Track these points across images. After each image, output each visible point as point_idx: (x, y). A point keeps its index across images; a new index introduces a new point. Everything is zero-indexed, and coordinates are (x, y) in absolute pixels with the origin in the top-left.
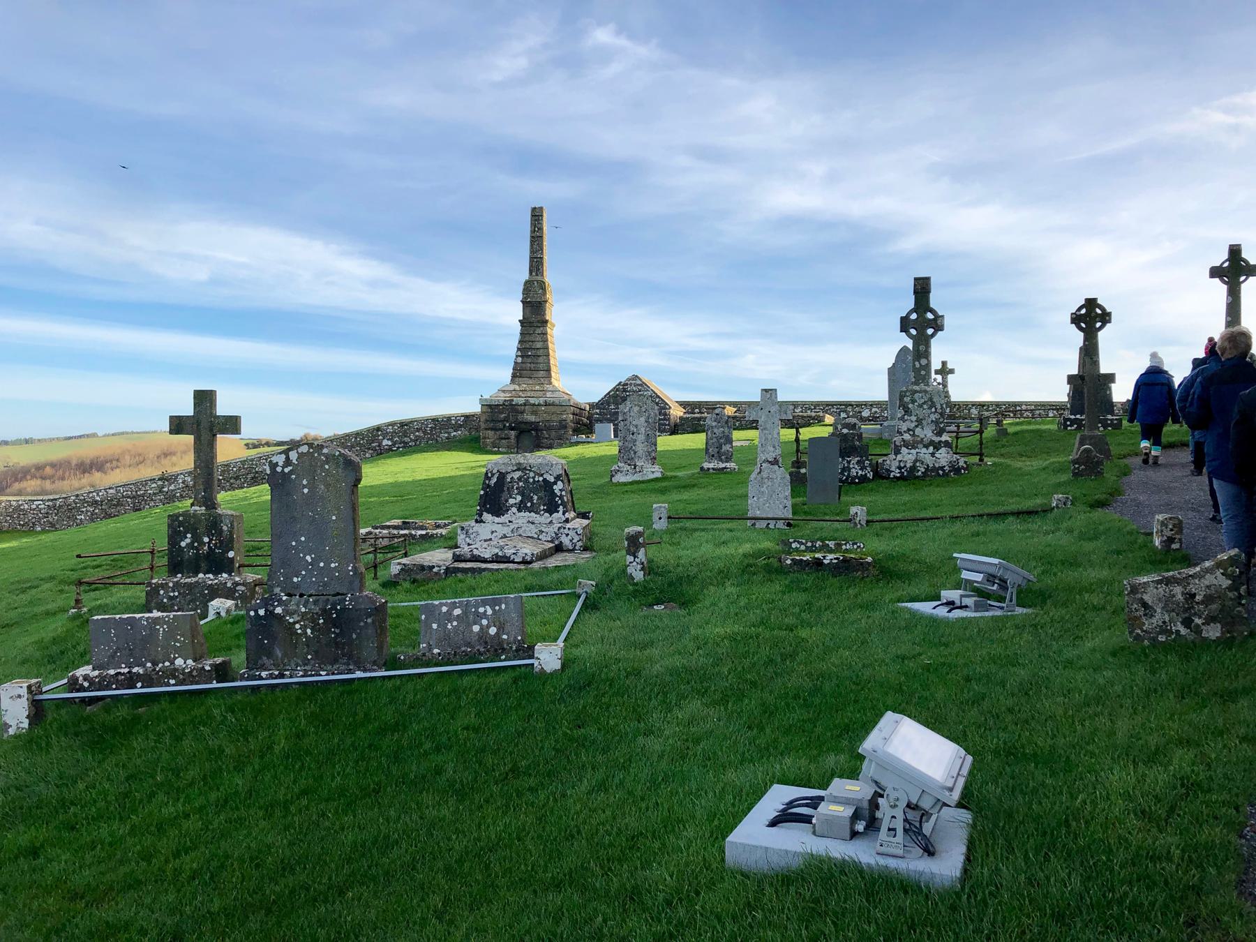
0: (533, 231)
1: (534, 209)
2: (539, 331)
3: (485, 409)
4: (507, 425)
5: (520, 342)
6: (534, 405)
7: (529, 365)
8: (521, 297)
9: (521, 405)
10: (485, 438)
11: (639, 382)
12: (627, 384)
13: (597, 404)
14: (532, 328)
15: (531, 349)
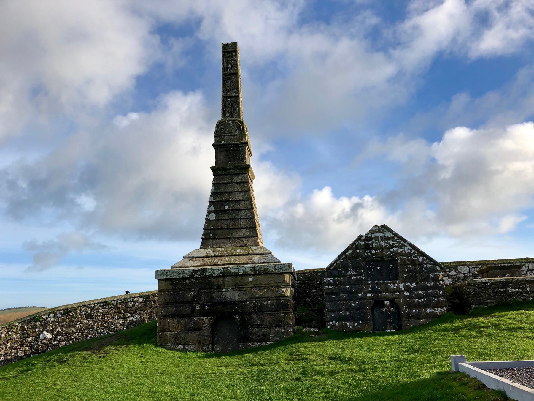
0: (225, 69)
1: (226, 47)
2: (237, 179)
3: (165, 285)
4: (198, 308)
5: (213, 194)
6: (237, 275)
7: (225, 222)
8: (213, 140)
9: (218, 276)
10: (163, 330)
11: (388, 235)
12: (370, 239)
13: (328, 268)
14: (229, 177)
15: (227, 202)
